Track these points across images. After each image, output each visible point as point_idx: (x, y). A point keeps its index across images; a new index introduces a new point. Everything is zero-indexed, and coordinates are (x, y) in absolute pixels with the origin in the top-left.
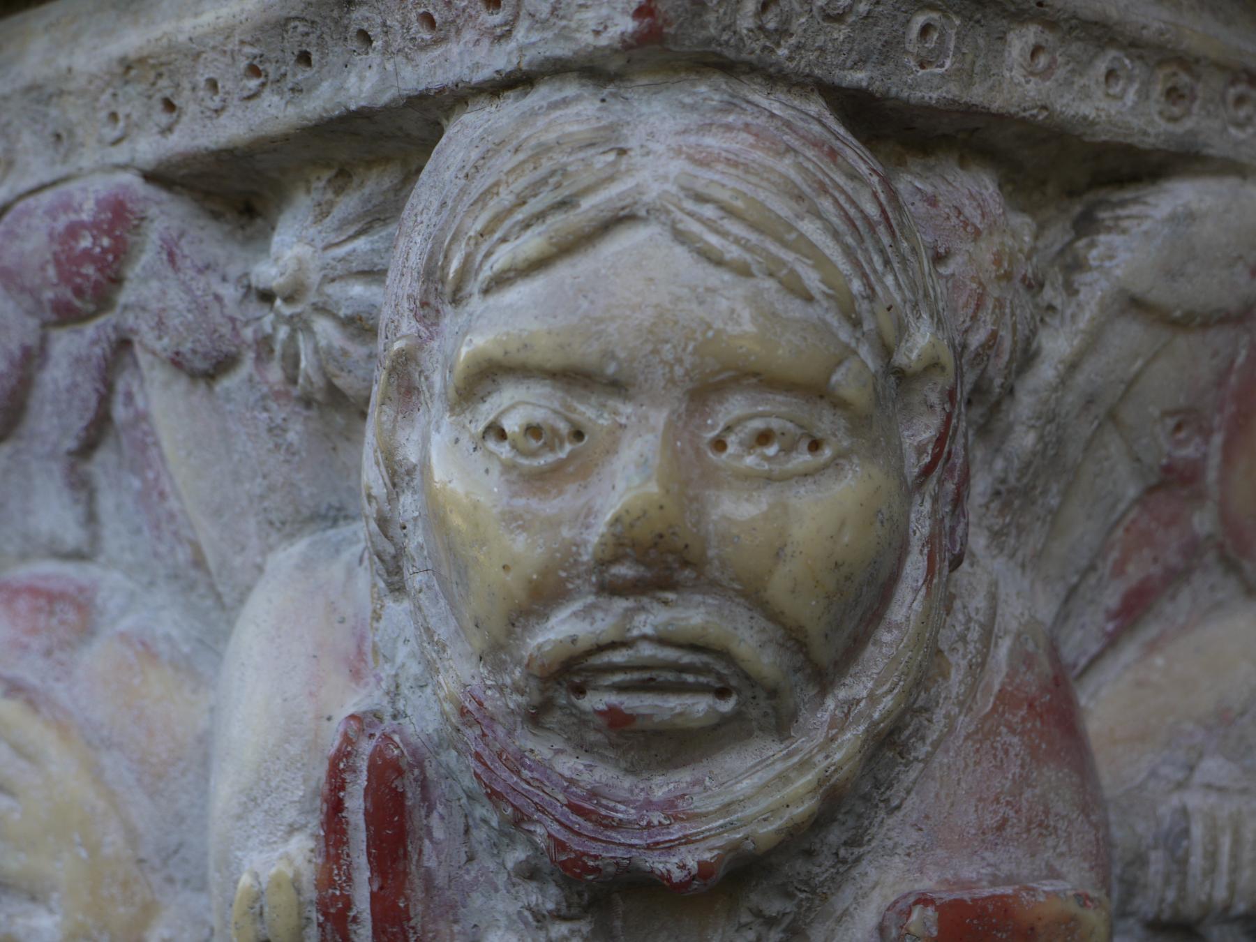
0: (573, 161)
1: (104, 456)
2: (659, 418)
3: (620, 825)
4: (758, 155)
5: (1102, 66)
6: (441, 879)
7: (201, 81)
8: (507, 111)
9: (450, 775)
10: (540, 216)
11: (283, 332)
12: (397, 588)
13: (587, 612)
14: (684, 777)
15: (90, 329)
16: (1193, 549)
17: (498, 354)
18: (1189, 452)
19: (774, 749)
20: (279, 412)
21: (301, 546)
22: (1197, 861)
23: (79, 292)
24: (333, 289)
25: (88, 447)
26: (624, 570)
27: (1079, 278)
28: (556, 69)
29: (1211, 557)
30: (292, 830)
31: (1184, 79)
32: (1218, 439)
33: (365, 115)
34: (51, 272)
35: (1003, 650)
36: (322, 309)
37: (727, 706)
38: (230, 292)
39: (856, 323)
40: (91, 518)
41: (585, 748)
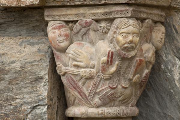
1: (85, 35)
12: (111, 43)
15: (87, 28)
21: (102, 41)
34: (85, 25)
40: (82, 39)
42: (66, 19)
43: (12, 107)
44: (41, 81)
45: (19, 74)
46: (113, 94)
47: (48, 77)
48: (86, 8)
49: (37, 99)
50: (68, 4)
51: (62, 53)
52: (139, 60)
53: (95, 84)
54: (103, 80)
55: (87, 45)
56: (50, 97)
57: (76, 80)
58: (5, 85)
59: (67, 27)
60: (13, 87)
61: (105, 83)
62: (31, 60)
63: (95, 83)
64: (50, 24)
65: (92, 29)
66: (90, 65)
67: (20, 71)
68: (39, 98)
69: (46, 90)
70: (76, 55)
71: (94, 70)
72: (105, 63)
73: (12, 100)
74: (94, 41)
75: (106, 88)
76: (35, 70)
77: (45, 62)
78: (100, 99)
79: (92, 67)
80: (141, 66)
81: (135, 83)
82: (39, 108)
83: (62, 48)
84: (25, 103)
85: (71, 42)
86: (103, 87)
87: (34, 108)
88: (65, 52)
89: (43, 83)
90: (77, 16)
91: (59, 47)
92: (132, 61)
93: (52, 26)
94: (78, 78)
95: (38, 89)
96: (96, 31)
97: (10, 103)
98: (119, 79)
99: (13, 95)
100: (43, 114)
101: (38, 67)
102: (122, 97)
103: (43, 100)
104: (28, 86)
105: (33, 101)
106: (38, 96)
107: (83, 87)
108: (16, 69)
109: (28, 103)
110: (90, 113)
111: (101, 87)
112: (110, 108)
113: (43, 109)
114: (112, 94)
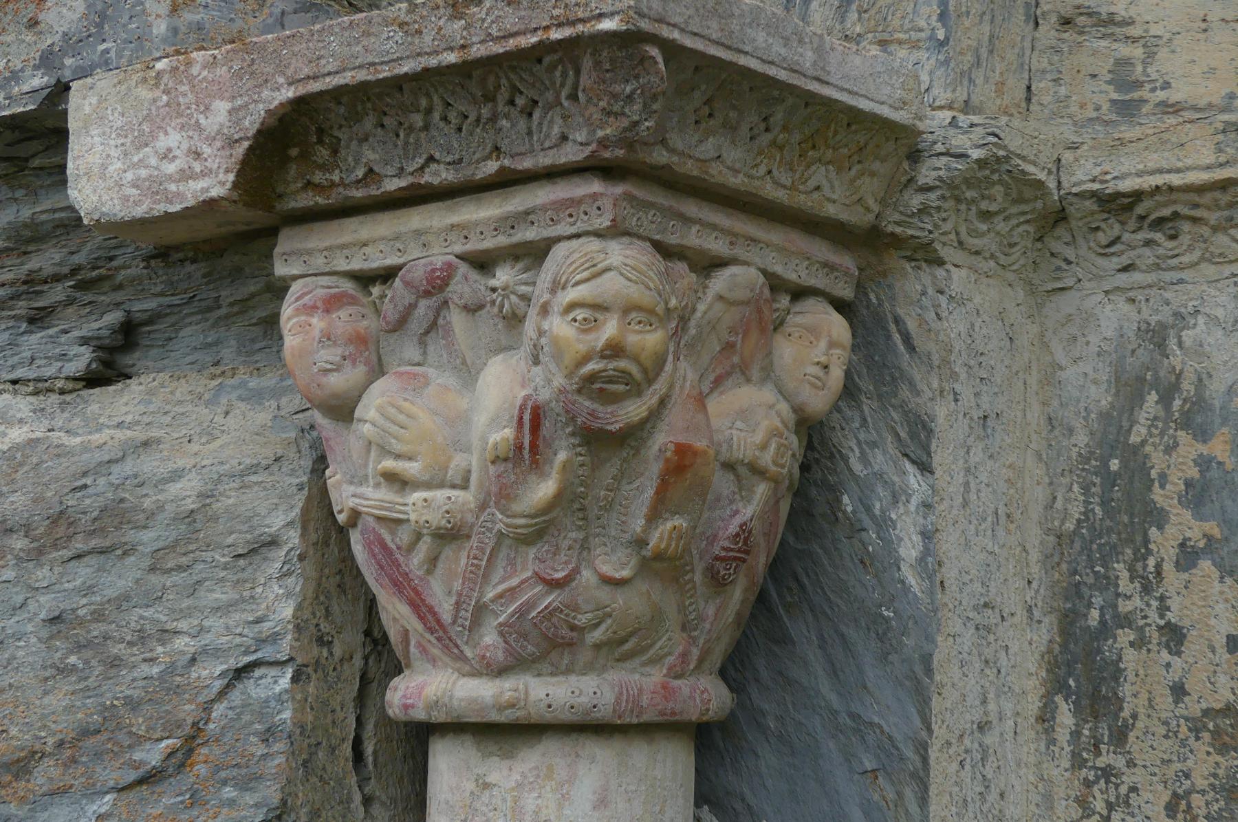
0: (595, 255)
1: (433, 334)
2: (616, 316)
3: (599, 418)
4: (638, 256)
5: (714, 235)
6: (548, 436)
7: (478, 231)
8: (574, 243)
9: (552, 409)
10: (588, 268)
11: (500, 299)
13: (597, 363)
14: (616, 406)
15: (434, 299)
16: (733, 366)
17: (576, 300)
18: (733, 339)
19: (638, 400)
20: (497, 321)
21: (501, 357)
22: (735, 447)
23: (434, 288)
24: (517, 287)
25: (427, 332)
26: (608, 353)
27: (707, 290)
28: (587, 233)
29: (737, 370)
30: (505, 427)
31: (734, 239)
32: (740, 336)
33: (531, 242)
34: (424, 282)
35: (688, 384)
36: (512, 293)
37: (628, 388)
38: (482, 288)
39: (661, 296)
40: (425, 353)
41: (591, 399)
42: (356, 265)
43: (155, 670)
44: (271, 555)
45: (190, 523)
46: (555, 610)
47: (302, 535)
48: (432, 207)
49: (251, 635)
50: (359, 194)
51: (343, 421)
52: (671, 447)
53: (472, 565)
54: (510, 547)
55: (440, 379)
56: (312, 628)
57: (399, 548)
58: (139, 574)
59: (365, 300)
60: (164, 585)
61: (519, 560)
62: (240, 464)
63: (475, 558)
64: (296, 288)
65: (457, 300)
66: (450, 473)
67: (192, 511)
68: (260, 632)
69: (288, 595)
70: (388, 425)
71: (466, 498)
72: (506, 460)
73: (159, 640)
74: (469, 362)
75: (523, 582)
76: (250, 507)
77: (293, 470)
78: (504, 631)
79: (458, 482)
80: (689, 476)
81: (659, 556)
82: (261, 678)
83: (335, 396)
84: (204, 651)
85: (378, 370)
86: (510, 577)
87: (241, 673)
88: (352, 419)
89: (278, 565)
90: (399, 245)
91: (319, 392)
92: (643, 452)
93: (297, 300)
94: (404, 536)
95: (259, 590)
96: (472, 309)
97: (151, 650)
98: (586, 539)
99: (164, 619)
100: (273, 704)
101: (262, 494)
102: (603, 627)
103: (275, 642)
104: (222, 580)
105: (237, 646)
106: (258, 621)
107: (430, 578)
108: (183, 503)
109: (215, 653)
110: (461, 700)
111: (503, 580)
112: (554, 679)
113: (276, 682)
114: (550, 613)
